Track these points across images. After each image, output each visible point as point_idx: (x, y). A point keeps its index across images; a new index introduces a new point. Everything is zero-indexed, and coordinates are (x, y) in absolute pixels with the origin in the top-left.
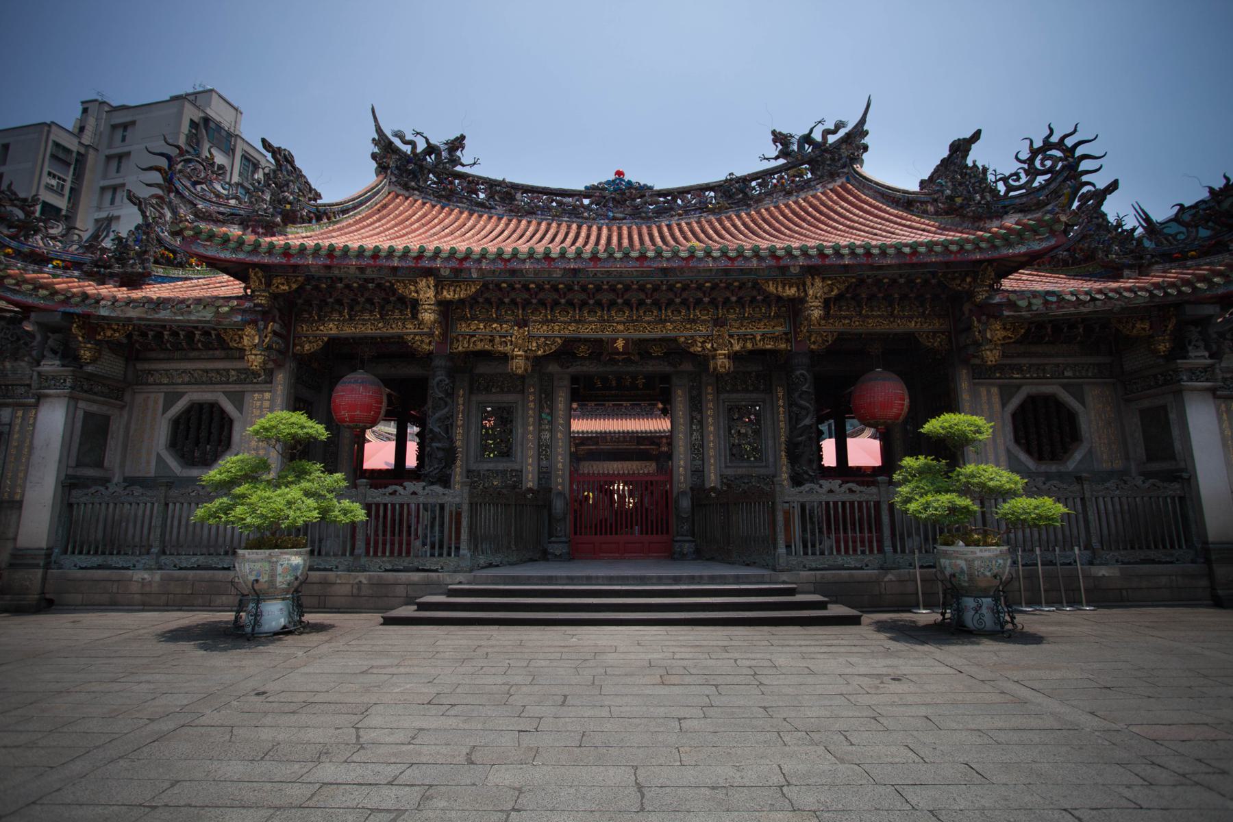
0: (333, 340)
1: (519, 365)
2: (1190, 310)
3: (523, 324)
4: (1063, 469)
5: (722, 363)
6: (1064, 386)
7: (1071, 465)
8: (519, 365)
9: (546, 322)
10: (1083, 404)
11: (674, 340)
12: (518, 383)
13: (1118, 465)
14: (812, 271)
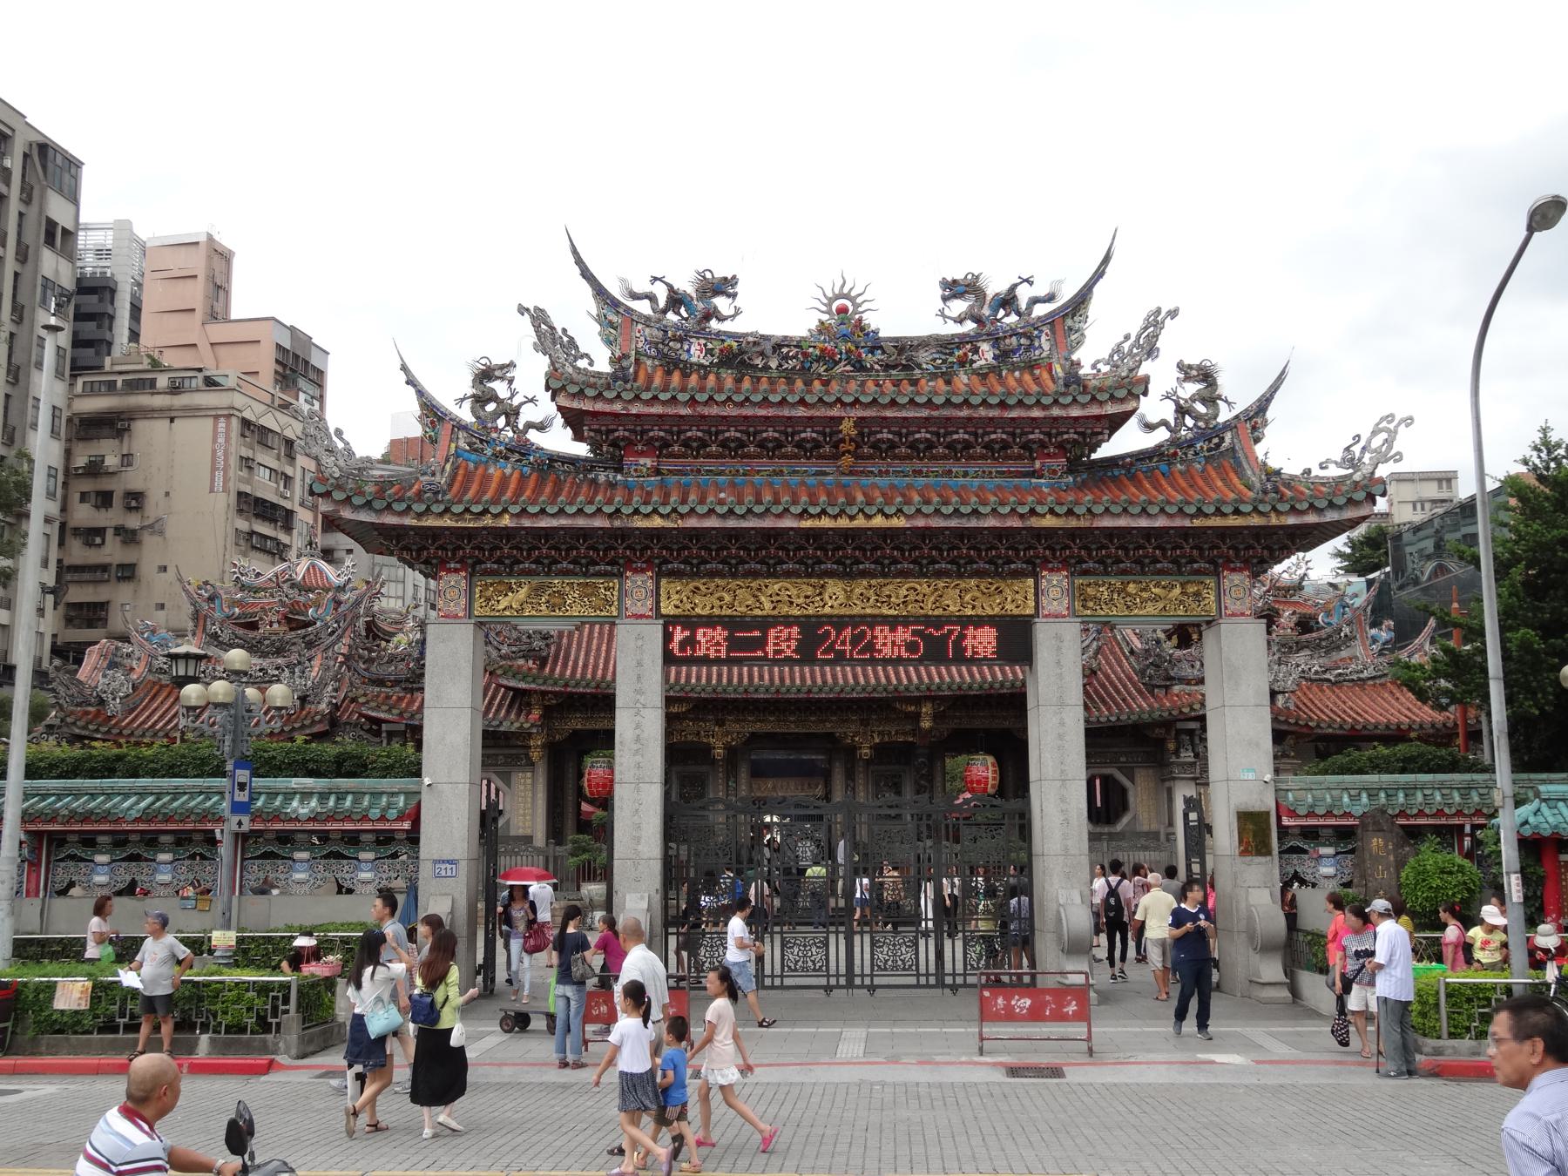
0: (575, 732)
1: (719, 752)
2: (1180, 725)
3: (720, 723)
4: (1112, 830)
5: (866, 752)
6: (1119, 769)
7: (1119, 827)
8: (719, 752)
9: (738, 721)
10: (1132, 781)
11: (832, 734)
12: (713, 762)
13: (1154, 827)
14: (927, 698)
